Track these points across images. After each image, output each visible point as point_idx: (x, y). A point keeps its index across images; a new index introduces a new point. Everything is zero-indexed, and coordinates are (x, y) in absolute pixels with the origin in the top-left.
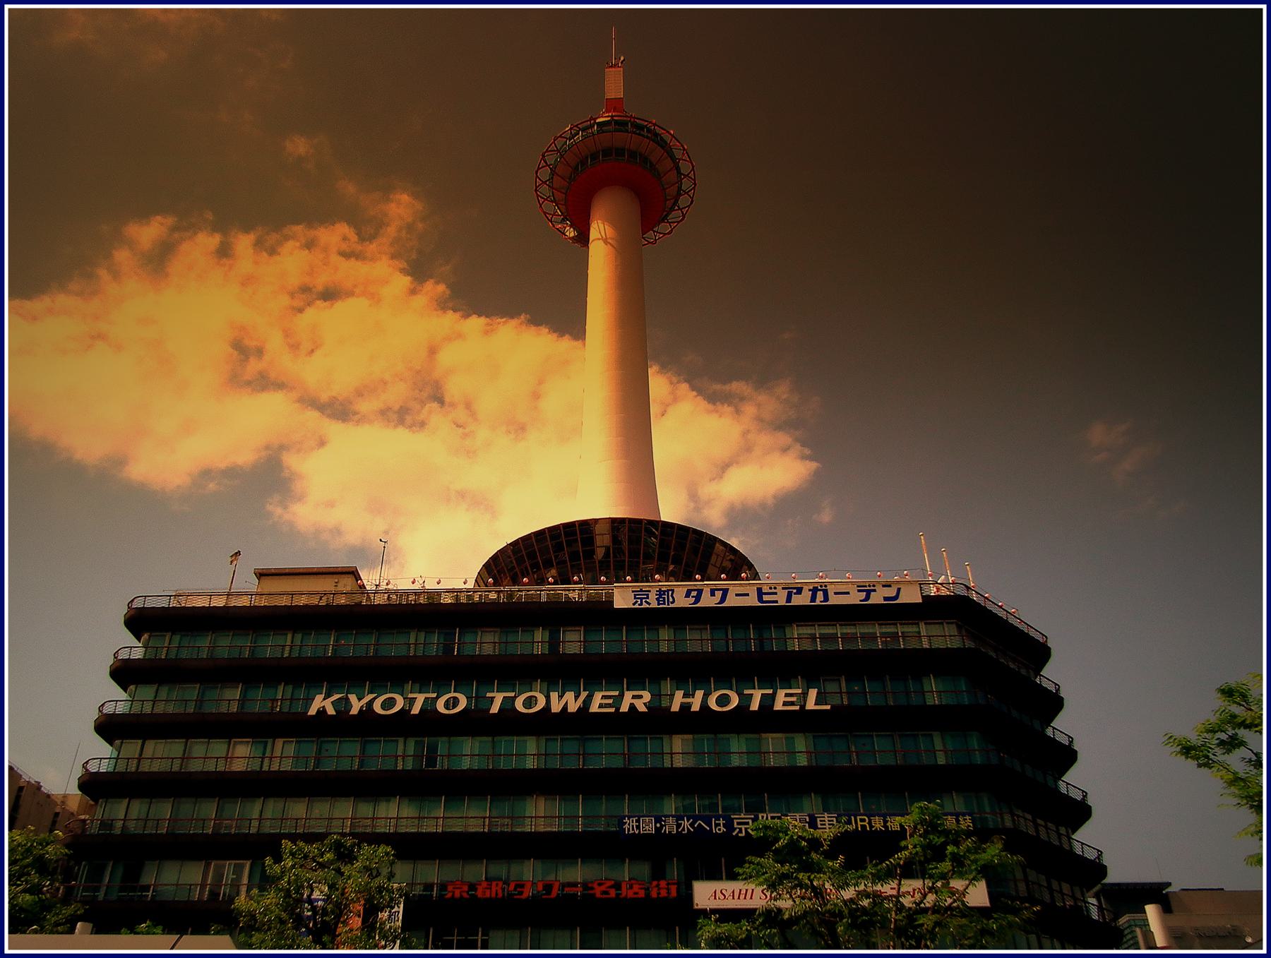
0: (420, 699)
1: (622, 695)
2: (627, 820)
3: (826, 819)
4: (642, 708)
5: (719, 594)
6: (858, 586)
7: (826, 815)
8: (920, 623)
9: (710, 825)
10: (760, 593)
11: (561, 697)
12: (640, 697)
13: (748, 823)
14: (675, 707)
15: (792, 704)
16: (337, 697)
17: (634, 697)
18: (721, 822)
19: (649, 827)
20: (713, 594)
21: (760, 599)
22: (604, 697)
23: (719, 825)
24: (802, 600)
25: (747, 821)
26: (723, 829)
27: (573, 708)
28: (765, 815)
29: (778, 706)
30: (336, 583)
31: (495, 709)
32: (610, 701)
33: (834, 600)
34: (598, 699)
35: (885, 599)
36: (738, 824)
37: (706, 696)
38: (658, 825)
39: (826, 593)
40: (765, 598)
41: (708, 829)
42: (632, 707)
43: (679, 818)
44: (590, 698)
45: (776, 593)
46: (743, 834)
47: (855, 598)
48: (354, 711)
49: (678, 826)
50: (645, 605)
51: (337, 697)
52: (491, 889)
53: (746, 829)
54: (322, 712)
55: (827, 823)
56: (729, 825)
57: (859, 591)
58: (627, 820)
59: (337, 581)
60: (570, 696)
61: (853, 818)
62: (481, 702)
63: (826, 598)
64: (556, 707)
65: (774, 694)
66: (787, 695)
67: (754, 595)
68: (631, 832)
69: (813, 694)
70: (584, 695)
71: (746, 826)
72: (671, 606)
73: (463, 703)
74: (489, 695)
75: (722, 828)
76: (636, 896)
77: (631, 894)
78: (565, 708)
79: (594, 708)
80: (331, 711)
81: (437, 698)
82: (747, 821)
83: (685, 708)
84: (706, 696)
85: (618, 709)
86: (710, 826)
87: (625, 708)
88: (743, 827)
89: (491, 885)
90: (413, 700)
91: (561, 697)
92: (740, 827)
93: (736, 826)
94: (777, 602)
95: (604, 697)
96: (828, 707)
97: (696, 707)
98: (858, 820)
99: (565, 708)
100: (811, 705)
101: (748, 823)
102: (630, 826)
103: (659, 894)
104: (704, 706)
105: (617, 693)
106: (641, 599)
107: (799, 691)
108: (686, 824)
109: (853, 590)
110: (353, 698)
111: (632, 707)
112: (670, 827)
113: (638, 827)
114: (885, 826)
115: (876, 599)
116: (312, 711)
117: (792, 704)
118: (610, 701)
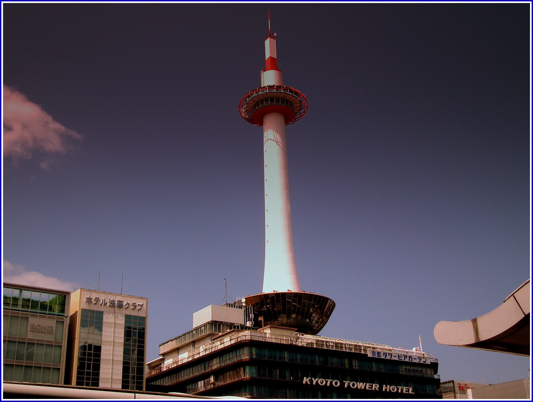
0: (329, 381)
1: (372, 386)
4: (377, 389)
5: (390, 355)
6: (418, 357)
10: (399, 356)
12: (376, 386)
16: (309, 378)
20: (389, 355)
21: (399, 359)
24: (407, 360)
33: (414, 361)
35: (424, 362)
39: (412, 358)
40: (400, 358)
45: (402, 357)
47: (417, 361)
48: (314, 383)
50: (375, 357)
51: (309, 378)
54: (306, 382)
57: (418, 359)
62: (343, 384)
63: (412, 360)
66: (406, 389)
67: (397, 356)
69: (411, 389)
72: (380, 358)
80: (309, 383)
81: (333, 381)
83: (386, 390)
87: (373, 389)
94: (402, 360)
97: (388, 390)
100: (410, 392)
106: (374, 354)
109: (417, 359)
110: (313, 379)
115: (422, 362)
116: (304, 382)
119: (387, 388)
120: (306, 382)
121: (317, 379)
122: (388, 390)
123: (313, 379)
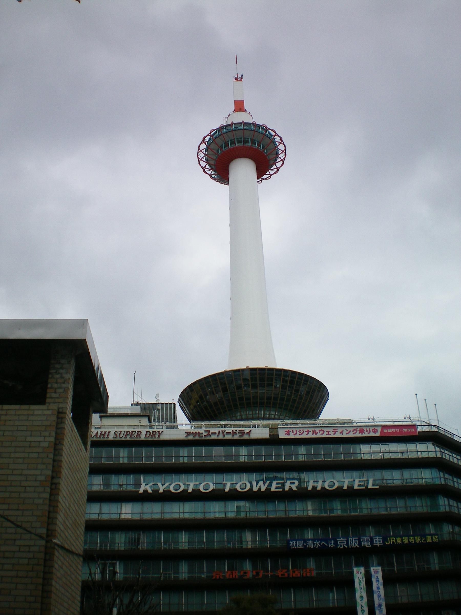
2: (291, 542)
3: (378, 539)
4: (295, 489)
7: (377, 538)
8: (417, 444)
9: (327, 543)
11: (257, 483)
12: (294, 483)
13: (344, 542)
14: (310, 488)
15: (362, 486)
17: (291, 483)
18: (333, 542)
19: (301, 545)
22: (277, 484)
23: (332, 543)
25: (343, 541)
27: (263, 489)
28: (351, 539)
29: (356, 487)
30: (140, 421)
31: (227, 490)
32: (280, 485)
34: (274, 485)
36: (340, 543)
37: (324, 482)
38: (305, 544)
41: (327, 545)
42: (291, 489)
43: (314, 540)
44: (270, 484)
46: (342, 547)
48: (161, 491)
49: (314, 544)
52: (232, 574)
53: (343, 545)
54: (145, 491)
55: (378, 541)
56: (336, 543)
58: (291, 542)
59: (140, 420)
60: (261, 483)
61: (389, 539)
64: (255, 489)
65: (354, 481)
66: (360, 481)
68: (293, 547)
70: (268, 482)
71: (344, 544)
73: (212, 487)
74: (224, 482)
75: (333, 544)
76: (297, 576)
77: (294, 575)
78: (259, 489)
79: (273, 489)
80: (150, 491)
82: (343, 541)
83: (314, 488)
84: (324, 482)
85: (284, 489)
86: (328, 544)
87: (287, 489)
88: (342, 544)
89: (232, 573)
90: (189, 485)
91: (257, 483)
92: (341, 544)
93: (339, 544)
95: (277, 484)
96: (378, 487)
97: (319, 488)
98: (391, 539)
99: (259, 489)
100: (370, 486)
101: (344, 542)
102: (293, 544)
103: (306, 575)
104: (323, 488)
105: (282, 481)
107: (365, 479)
108: (317, 543)
110: (160, 484)
111: (291, 489)
112: (310, 544)
113: (296, 545)
114: (402, 542)
116: (141, 491)
117: (362, 486)
118: (280, 485)
119: (315, 484)
120: (145, 491)
121: (167, 484)
122: (319, 488)
123: (160, 484)
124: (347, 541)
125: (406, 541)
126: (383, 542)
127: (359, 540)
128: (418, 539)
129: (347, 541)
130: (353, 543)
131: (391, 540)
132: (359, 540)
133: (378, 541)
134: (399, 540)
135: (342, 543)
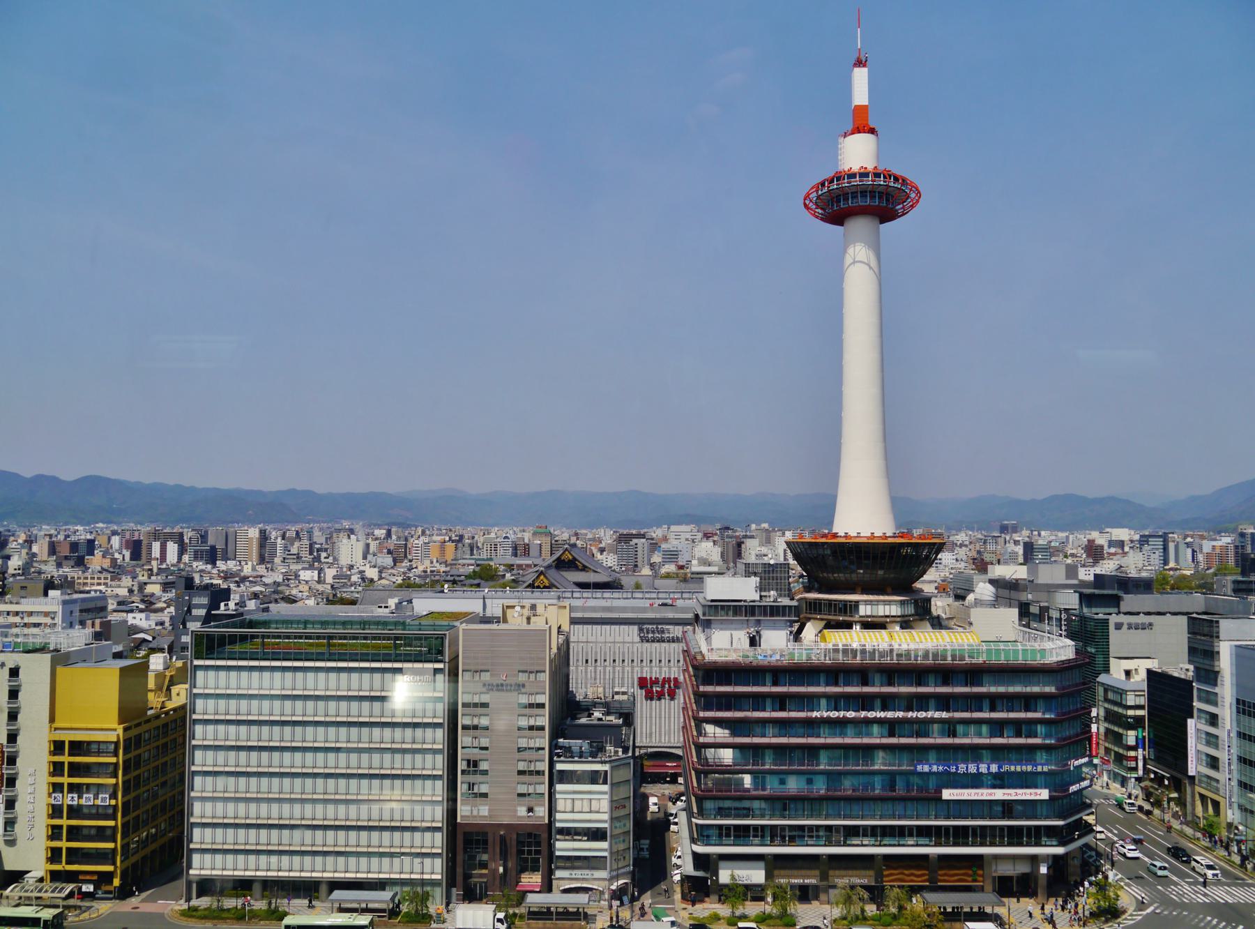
9: (949, 768)
19: (926, 768)
26: (954, 770)
56: (957, 769)
86: (949, 768)
112: (935, 768)
124: (967, 768)
125: (1019, 769)
126: (999, 769)
127: (978, 766)
128: (1029, 768)
129: (967, 768)
130: (972, 769)
131: (1006, 768)
132: (978, 766)
133: (994, 768)
134: (1013, 768)
135: (962, 768)
